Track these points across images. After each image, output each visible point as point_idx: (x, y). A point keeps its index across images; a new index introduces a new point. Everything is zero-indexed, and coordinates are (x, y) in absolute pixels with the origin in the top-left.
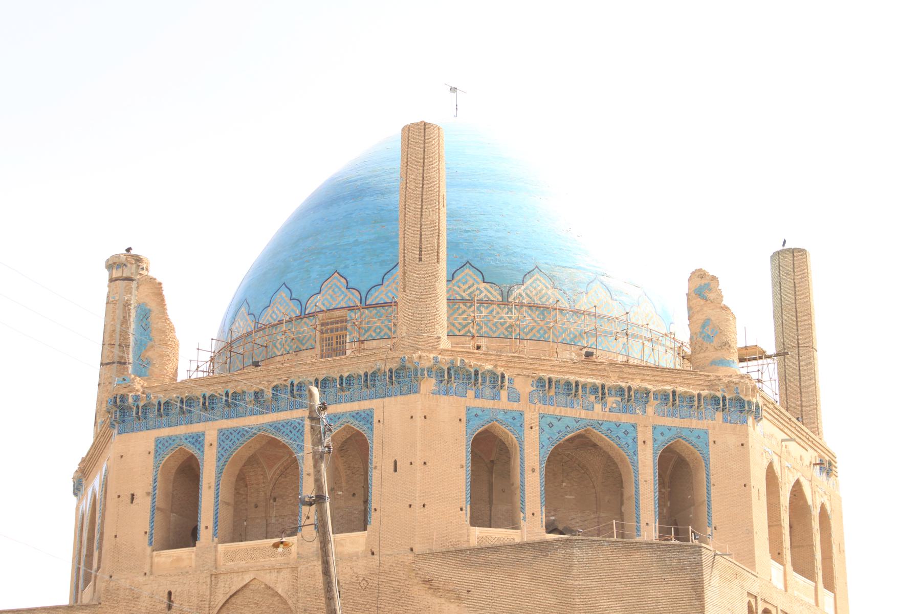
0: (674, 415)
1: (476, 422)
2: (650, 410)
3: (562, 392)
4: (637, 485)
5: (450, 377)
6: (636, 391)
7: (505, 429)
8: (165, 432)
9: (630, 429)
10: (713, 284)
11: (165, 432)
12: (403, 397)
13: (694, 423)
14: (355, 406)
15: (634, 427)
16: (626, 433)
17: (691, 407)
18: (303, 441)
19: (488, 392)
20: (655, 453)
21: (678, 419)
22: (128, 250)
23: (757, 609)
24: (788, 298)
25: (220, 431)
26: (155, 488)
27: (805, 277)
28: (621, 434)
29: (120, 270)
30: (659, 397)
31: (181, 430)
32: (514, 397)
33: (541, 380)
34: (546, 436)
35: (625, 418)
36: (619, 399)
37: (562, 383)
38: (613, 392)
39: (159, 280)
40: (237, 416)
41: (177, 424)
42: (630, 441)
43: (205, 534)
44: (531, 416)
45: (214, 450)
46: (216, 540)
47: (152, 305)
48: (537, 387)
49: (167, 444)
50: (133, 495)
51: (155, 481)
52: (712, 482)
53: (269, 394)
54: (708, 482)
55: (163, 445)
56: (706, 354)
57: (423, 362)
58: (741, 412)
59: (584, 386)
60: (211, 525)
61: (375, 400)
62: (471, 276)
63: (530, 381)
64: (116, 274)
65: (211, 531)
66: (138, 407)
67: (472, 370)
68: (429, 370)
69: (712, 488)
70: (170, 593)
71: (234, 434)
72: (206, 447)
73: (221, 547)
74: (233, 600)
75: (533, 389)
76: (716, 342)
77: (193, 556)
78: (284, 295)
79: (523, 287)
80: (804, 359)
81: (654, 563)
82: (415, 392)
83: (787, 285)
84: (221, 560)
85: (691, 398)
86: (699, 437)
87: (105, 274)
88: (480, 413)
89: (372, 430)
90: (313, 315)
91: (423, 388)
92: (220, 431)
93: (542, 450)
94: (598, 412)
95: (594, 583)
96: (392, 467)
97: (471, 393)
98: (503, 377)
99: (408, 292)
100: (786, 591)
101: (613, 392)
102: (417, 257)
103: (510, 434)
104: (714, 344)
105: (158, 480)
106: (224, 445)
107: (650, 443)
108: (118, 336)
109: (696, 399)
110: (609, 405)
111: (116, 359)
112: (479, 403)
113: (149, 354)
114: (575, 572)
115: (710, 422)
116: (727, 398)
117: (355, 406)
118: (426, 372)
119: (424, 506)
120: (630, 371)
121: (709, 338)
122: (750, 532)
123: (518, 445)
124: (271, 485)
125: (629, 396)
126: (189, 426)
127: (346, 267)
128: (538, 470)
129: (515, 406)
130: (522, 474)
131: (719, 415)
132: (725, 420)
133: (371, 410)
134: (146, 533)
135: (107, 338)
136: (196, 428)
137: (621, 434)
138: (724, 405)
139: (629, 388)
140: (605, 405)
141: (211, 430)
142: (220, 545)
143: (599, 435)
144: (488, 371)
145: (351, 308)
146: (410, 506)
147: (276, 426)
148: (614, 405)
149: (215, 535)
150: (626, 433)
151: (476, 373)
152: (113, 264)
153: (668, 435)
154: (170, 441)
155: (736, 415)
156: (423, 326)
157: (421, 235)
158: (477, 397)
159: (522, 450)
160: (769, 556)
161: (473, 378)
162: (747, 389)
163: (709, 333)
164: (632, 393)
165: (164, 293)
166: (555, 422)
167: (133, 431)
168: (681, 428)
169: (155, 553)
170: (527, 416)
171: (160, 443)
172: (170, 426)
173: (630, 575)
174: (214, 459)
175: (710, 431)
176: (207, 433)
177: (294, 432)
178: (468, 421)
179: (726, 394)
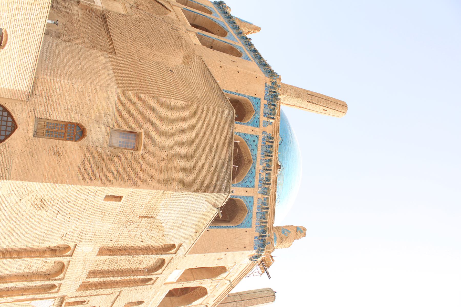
2: (260, 196)
3: (268, 149)
6: (268, 188)
9: (252, 184)
10: (303, 234)
13: (254, 220)
17: (261, 218)
19: (267, 111)
20: (242, 197)
23: (169, 254)
24: (258, 295)
27: (266, 302)
28: (250, 179)
30: (265, 201)
32: (265, 124)
33: (272, 138)
34: (250, 138)
35: (257, 182)
36: (264, 179)
38: (267, 176)
42: (247, 183)
44: (258, 131)
52: (229, 229)
54: (229, 227)
57: (279, 80)
58: (259, 246)
59: (270, 160)
63: (271, 133)
67: (275, 104)
68: (274, 83)
69: (227, 229)
74: (159, 4)
76: (283, 235)
80: (237, 303)
81: (221, 161)
83: (263, 294)
85: (265, 218)
86: (249, 222)
88: (258, 105)
94: (260, 167)
95: (211, 119)
97: (266, 102)
98: (273, 119)
100: (165, 284)
103: (250, 119)
107: (246, 194)
110: (262, 173)
112: (262, 106)
114: (217, 108)
116: (266, 238)
118: (274, 81)
120: (274, 187)
122: (206, 251)
129: (261, 124)
131: (257, 234)
132: (255, 238)
139: (270, 184)
140: (262, 172)
143: (250, 168)
144: (275, 112)
148: (262, 176)
150: (251, 182)
153: (250, 205)
155: (257, 243)
160: (187, 268)
162: (270, 248)
164: (267, 186)
166: (255, 143)
173: (215, 144)
178: (255, 98)
179: (267, 237)
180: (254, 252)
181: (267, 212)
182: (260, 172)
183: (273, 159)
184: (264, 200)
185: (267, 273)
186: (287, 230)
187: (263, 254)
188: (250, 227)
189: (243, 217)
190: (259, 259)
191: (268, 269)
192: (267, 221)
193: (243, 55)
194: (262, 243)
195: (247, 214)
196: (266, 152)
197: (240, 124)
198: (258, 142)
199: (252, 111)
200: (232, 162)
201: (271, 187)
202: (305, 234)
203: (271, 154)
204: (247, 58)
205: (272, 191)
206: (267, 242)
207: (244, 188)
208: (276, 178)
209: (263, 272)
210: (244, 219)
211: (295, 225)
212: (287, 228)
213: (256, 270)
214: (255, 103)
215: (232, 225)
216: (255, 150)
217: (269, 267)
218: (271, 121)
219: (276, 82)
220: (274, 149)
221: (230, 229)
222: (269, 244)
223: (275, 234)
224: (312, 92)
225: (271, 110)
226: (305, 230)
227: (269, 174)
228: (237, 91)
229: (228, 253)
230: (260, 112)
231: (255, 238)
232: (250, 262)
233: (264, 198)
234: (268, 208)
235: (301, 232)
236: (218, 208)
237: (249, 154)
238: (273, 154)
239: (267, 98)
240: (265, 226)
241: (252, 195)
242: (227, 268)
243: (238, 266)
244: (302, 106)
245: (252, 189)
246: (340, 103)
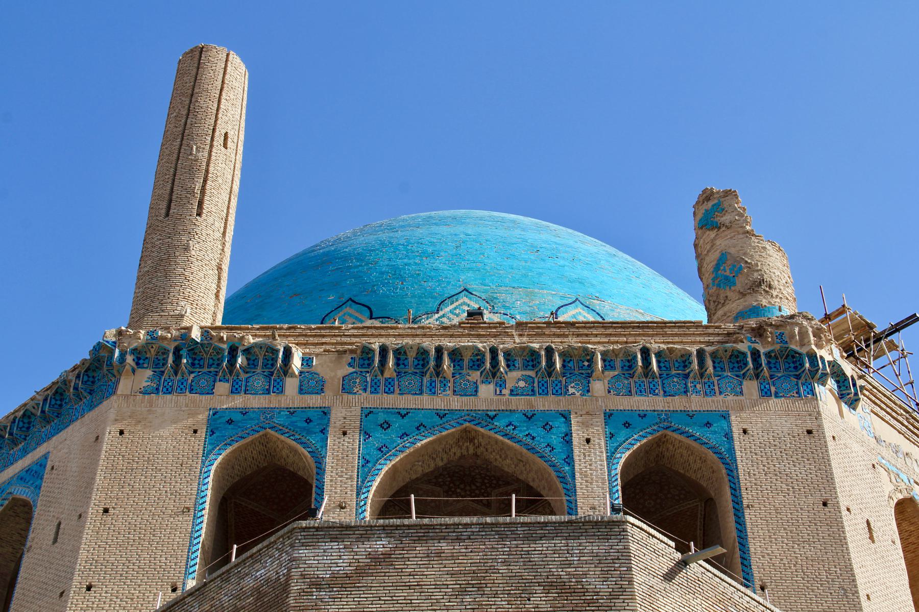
0: (653, 392)
2: (598, 387)
3: (411, 369)
7: (289, 441)
13: (696, 402)
15: (566, 416)
17: (687, 376)
19: (259, 382)
33: (367, 352)
36: (532, 373)
38: (519, 362)
48: (362, 366)
52: (745, 502)
56: (726, 308)
58: (798, 377)
59: (455, 355)
62: (351, 316)
63: (348, 358)
68: (140, 356)
69: (747, 512)
75: (351, 370)
76: (740, 283)
79: (437, 316)
85: (685, 360)
88: (237, 417)
96: (52, 537)
97: (222, 387)
98: (288, 353)
101: (519, 362)
102: (163, 212)
103: (300, 448)
104: (739, 287)
110: (510, 385)
112: (239, 401)
115: (731, 398)
116: (762, 351)
118: (130, 359)
121: (728, 282)
125: (551, 363)
129: (314, 401)
131: (751, 387)
138: (757, 365)
139: (549, 351)
140: (502, 384)
148: (522, 384)
156: (156, 304)
157: (173, 184)
158: (234, 391)
162: (803, 334)
163: (728, 273)
168: (669, 414)
170: (338, 415)
180: (826, 393)
181: (659, 354)
182: (506, 392)
183: (449, 343)
184: (613, 368)
185: (896, 328)
186: (717, 267)
187: (828, 358)
189: (688, 448)
190: (849, 369)
191: (878, 330)
192: (694, 349)
193: (22, 492)
194: (784, 366)
196: (423, 374)
197: (321, 488)
198: (387, 410)
199: (265, 441)
200: (501, 519)
201: (558, 344)
202: (728, 193)
203: (433, 352)
204: (35, 474)
205: (574, 342)
206: (777, 347)
207: (576, 451)
208: (519, 325)
209: (892, 347)
210: (694, 444)
211: (691, 236)
212: (709, 266)
213: (887, 372)
214: (230, 430)
215: (728, 491)
216: (420, 417)
217: (871, 327)
218: (297, 363)
219: (134, 351)
220: (409, 341)
222: (786, 338)
223: (740, 315)
224: (156, 197)
225: (252, 362)
226: (707, 196)
227: (508, 354)
229: (843, 503)
230: (263, 411)
231: (765, 394)
232: (864, 404)
233: (605, 368)
234: (645, 352)
235: (719, 209)
236: (684, 563)
237: (438, 441)
238: (429, 344)
239: (203, 383)
240: (714, 355)
242: (901, 497)
243: (885, 453)
244: (218, 235)
246: (189, 79)
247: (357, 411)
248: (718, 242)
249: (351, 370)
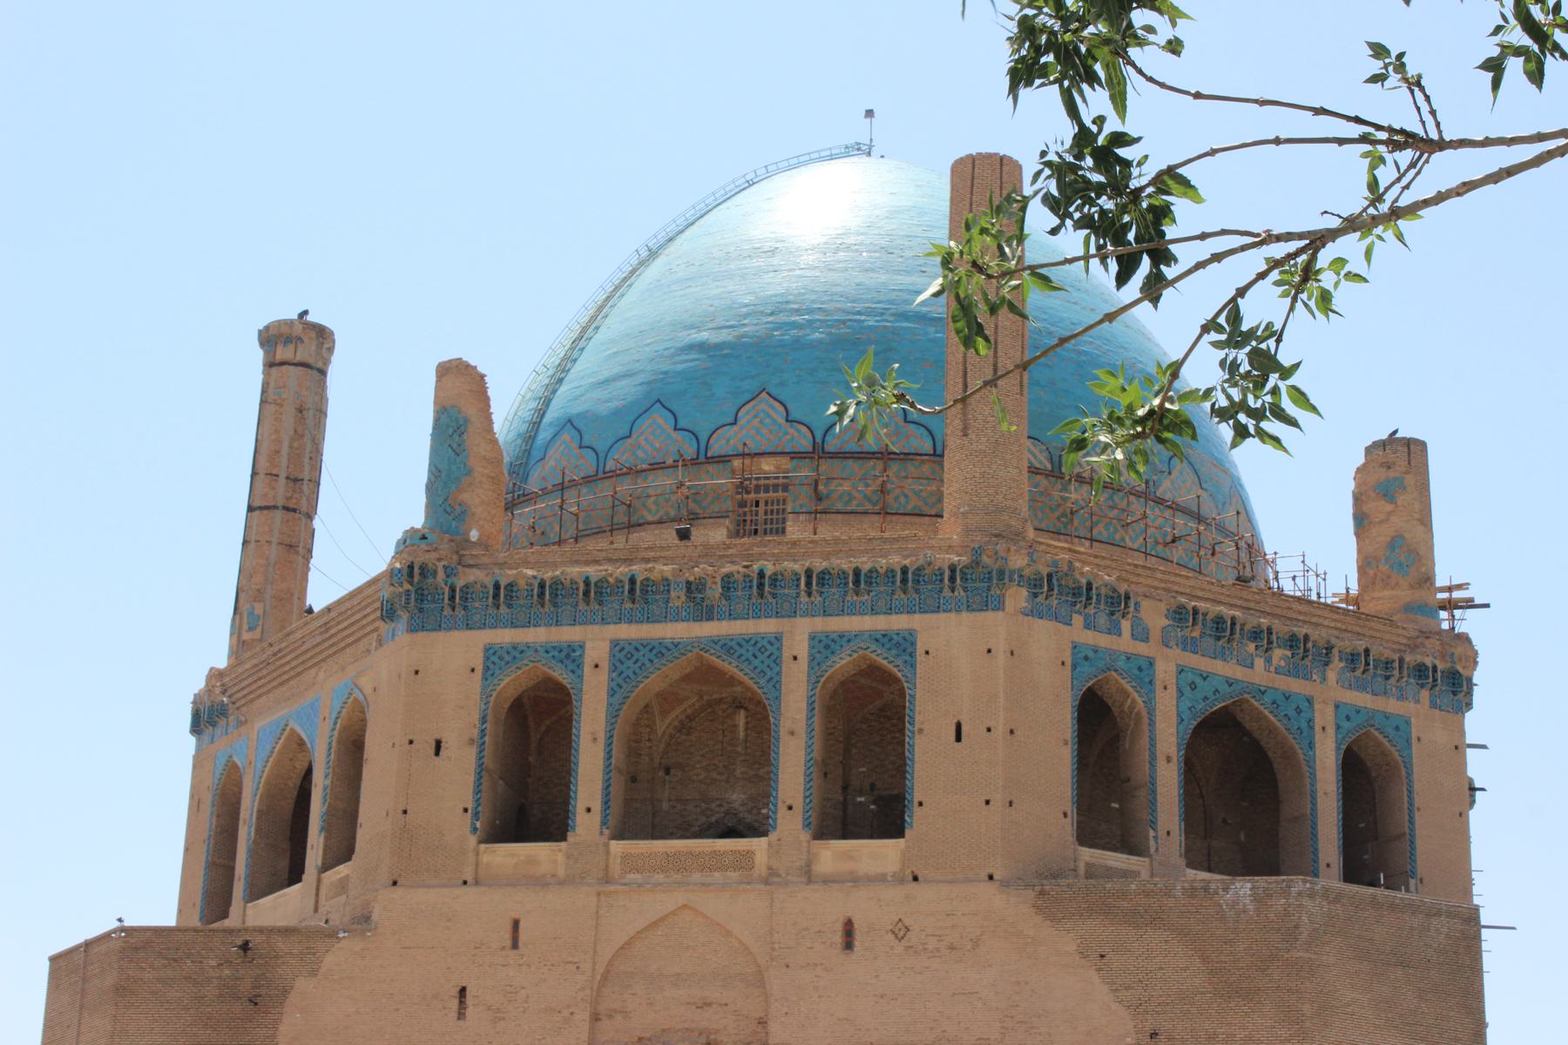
1: (1086, 668)
2: (1332, 675)
4: (1314, 798)
5: (1051, 589)
8: (505, 636)
11: (505, 636)
12: (972, 616)
13: (1392, 706)
14: (880, 623)
15: (1310, 701)
16: (1298, 710)
17: (1387, 678)
18: (779, 673)
19: (1102, 620)
20: (1338, 748)
21: (1369, 696)
22: (306, 312)
25: (615, 643)
26: (483, 733)
28: (1292, 713)
29: (291, 347)
31: (537, 635)
32: (1141, 635)
35: (1296, 686)
36: (1289, 653)
37: (1209, 617)
39: (481, 369)
40: (649, 619)
41: (527, 624)
42: (1304, 725)
43: (587, 819)
44: (1165, 670)
45: (603, 676)
46: (606, 832)
47: (471, 412)
49: (507, 658)
50: (438, 744)
51: (484, 720)
53: (715, 591)
54: (1411, 804)
55: (501, 658)
60: (597, 807)
61: (917, 616)
63: (1163, 607)
64: (283, 353)
65: (596, 816)
66: (453, 589)
67: (1084, 581)
70: (516, 924)
71: (643, 651)
72: (587, 669)
73: (617, 847)
75: (1167, 622)
77: (560, 858)
78: (660, 421)
82: (995, 609)
84: (616, 868)
86: (1397, 728)
87: (258, 355)
88: (1091, 655)
89: (913, 666)
90: (723, 459)
91: (1009, 603)
92: (615, 643)
93: (1181, 727)
97: (1078, 620)
99: (972, 436)
105: (489, 718)
106: (621, 668)
107: (1331, 731)
108: (284, 461)
109: (1396, 665)
110: (1275, 661)
111: (280, 504)
112: (1090, 638)
113: (465, 496)
115: (1412, 705)
117: (880, 623)
119: (1011, 804)
123: (1144, 713)
124: (662, 746)
126: (553, 629)
127: (782, 384)
128: (1175, 759)
129: (1142, 648)
130: (1153, 764)
132: (1433, 705)
133: (912, 632)
134: (466, 810)
135: (263, 464)
136: (568, 634)
137: (1292, 713)
140: (1269, 660)
141: (596, 641)
142: (613, 843)
145: (795, 455)
146: (987, 802)
147: (727, 646)
149: (603, 823)
150: (1298, 710)
151: (1089, 586)
152: (273, 338)
154: (516, 653)
158: (1087, 627)
159: (1152, 723)
161: (1083, 594)
165: (490, 393)
166: (1198, 680)
167: (439, 628)
169: (483, 846)
171: (494, 659)
172: (514, 625)
174: (604, 694)
175: (1413, 721)
176: (588, 645)
177: (761, 657)
178: (1074, 667)
179: (1437, 662)
188: (1408, 723)
189: (1379, 745)
195: (1376, 733)
214: (1086, 668)
221: (1417, 802)
228: (1066, 743)
231: (1433, 705)
241: (1330, 709)
245: (1317, 706)
247: (1173, 668)
248: (1394, 519)
249: (1167, 622)
